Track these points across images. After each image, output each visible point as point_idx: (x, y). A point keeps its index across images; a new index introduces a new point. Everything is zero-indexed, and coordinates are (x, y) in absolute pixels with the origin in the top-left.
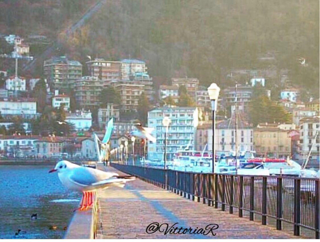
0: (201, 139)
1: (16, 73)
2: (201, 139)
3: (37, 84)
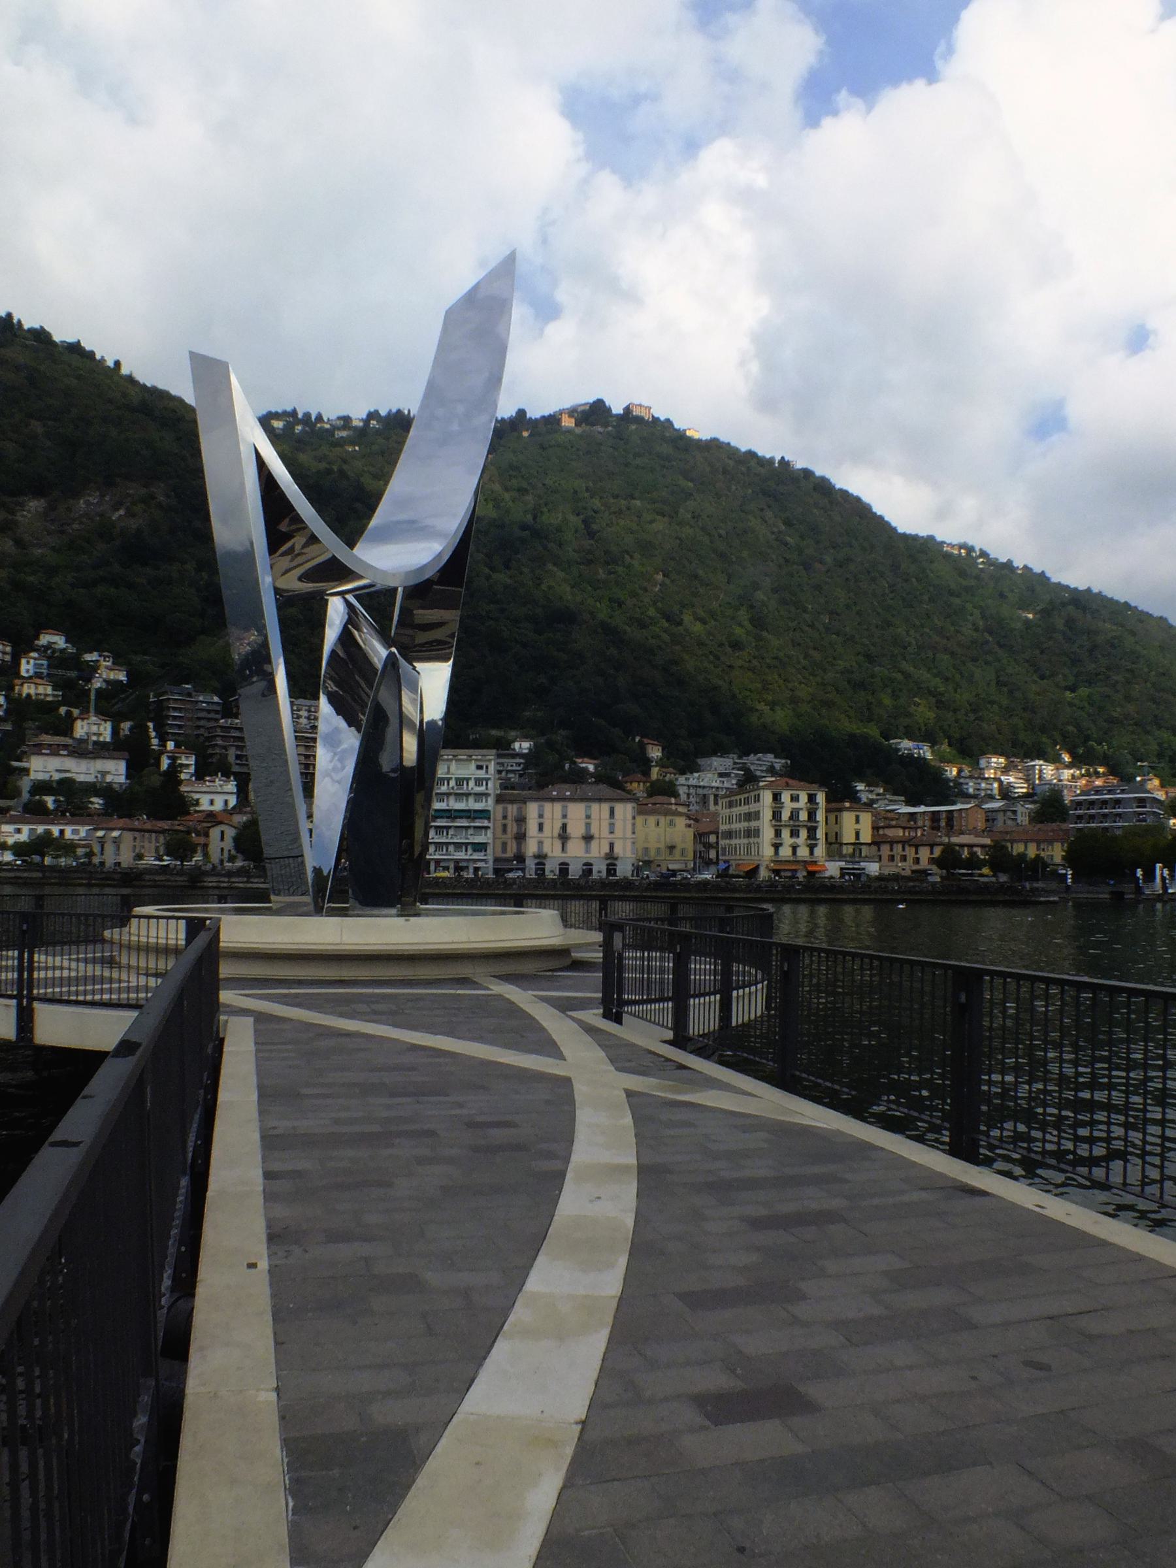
0: (505, 826)
1: (92, 709)
2: (505, 826)
3: (131, 729)
